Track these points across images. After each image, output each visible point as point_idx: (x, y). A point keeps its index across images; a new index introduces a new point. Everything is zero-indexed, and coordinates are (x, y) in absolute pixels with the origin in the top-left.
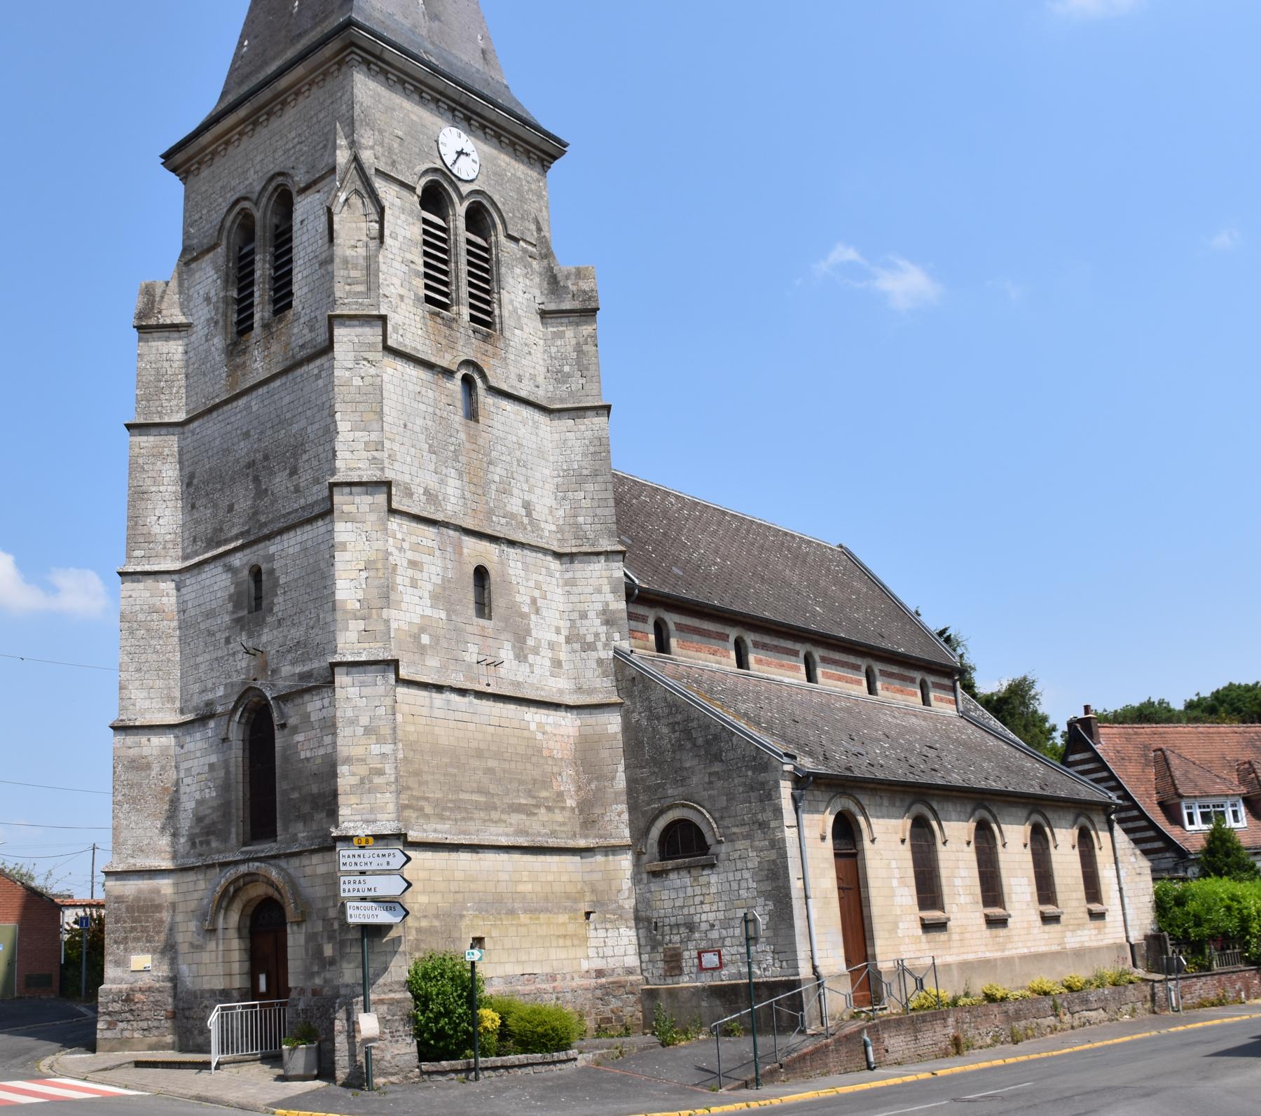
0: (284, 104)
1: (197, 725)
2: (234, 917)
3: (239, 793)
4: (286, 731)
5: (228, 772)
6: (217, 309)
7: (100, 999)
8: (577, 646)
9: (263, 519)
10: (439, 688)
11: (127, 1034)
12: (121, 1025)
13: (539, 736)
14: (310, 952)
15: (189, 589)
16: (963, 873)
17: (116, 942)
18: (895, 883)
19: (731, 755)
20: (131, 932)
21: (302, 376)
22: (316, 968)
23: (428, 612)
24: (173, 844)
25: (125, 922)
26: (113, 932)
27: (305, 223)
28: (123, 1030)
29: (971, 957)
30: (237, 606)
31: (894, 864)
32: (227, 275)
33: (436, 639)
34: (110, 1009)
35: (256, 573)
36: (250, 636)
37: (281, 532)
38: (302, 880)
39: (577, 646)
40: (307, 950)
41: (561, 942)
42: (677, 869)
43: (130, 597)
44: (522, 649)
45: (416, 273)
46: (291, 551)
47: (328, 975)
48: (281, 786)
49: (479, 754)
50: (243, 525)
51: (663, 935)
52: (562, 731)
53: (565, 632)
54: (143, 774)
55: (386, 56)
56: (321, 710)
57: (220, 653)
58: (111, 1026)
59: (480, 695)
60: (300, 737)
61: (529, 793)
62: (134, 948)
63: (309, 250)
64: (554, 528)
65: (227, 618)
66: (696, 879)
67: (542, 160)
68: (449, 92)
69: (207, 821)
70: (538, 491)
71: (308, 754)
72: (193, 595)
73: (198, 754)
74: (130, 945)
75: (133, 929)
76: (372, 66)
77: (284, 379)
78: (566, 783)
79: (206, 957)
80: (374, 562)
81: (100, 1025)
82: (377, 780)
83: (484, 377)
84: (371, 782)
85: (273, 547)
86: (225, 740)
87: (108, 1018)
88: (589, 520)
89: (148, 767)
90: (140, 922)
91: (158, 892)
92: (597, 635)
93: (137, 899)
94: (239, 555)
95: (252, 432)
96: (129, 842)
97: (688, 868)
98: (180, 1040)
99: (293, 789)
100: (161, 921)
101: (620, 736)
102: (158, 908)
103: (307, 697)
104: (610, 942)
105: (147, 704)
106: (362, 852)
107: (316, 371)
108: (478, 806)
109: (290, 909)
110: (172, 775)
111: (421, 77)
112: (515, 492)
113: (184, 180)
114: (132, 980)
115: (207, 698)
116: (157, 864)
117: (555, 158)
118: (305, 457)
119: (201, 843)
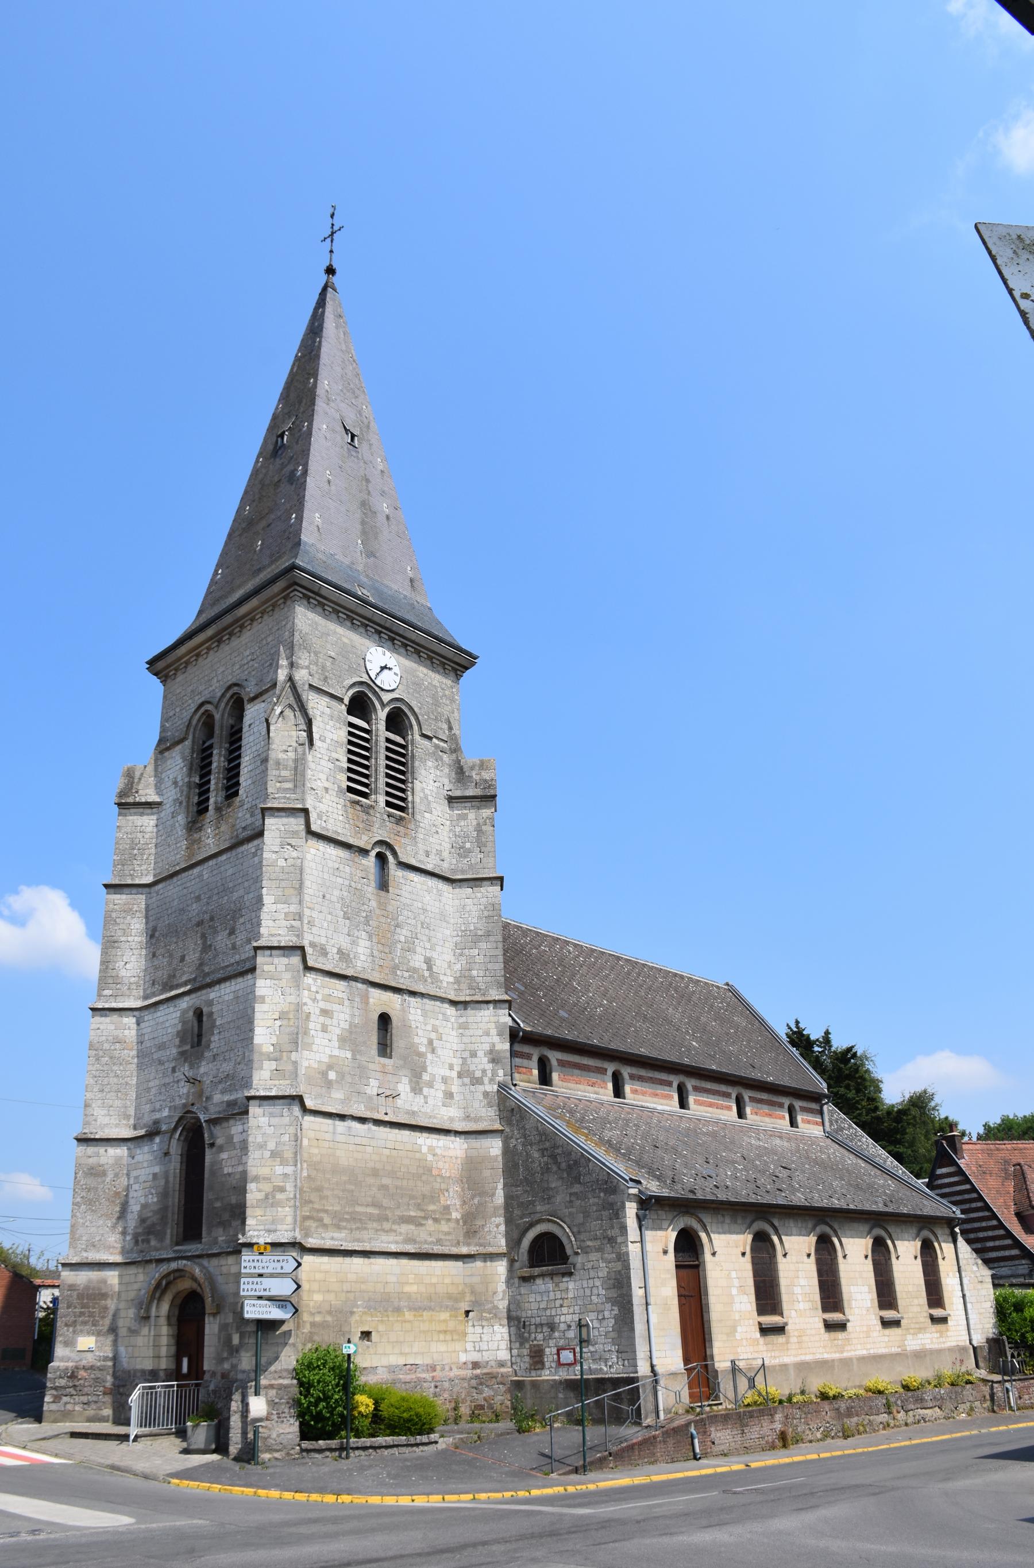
0: (242, 627)
1: (146, 1139)
2: (165, 1307)
3: (175, 1200)
4: (214, 1149)
5: (167, 1182)
6: (182, 792)
7: (49, 1375)
8: (467, 1080)
9: (207, 969)
10: (342, 1117)
11: (69, 1407)
12: (65, 1399)
13: (430, 1158)
15: (147, 1024)
16: (803, 1282)
17: (66, 1325)
18: (734, 1291)
19: (587, 1179)
20: (80, 1316)
21: (242, 852)
22: (225, 1355)
23: (336, 1052)
25: (75, 1307)
26: (65, 1316)
27: (252, 726)
28: (66, 1403)
29: (808, 1358)
30: (183, 1041)
31: (734, 1274)
32: (191, 764)
33: (341, 1075)
34: (57, 1384)
35: (199, 1014)
36: (191, 1067)
37: (220, 981)
38: (219, 1277)
39: (467, 1080)
40: (219, 1338)
41: (442, 1337)
42: (542, 1275)
43: (99, 1029)
44: (418, 1083)
45: (341, 769)
46: (226, 998)
47: (234, 1361)
48: (208, 1195)
49: (375, 1173)
50: (191, 973)
51: (530, 1333)
52: (451, 1153)
53: (457, 1068)
54: (100, 1180)
55: (323, 592)
57: (167, 1080)
58: (57, 1399)
59: (378, 1122)
60: (224, 1156)
61: (419, 1207)
62: (81, 1331)
63: (254, 749)
64: (451, 980)
65: (174, 1051)
66: (557, 1285)
67: (455, 670)
68: (376, 619)
69: (149, 1222)
70: (438, 949)
71: (230, 1170)
72: (149, 1030)
73: (145, 1165)
74: (79, 1327)
75: (82, 1314)
76: (312, 600)
78: (453, 1198)
79: (140, 1341)
80: (287, 1013)
81: (47, 1399)
82: (279, 1196)
83: (394, 853)
84: (274, 1197)
85: (213, 994)
86: (167, 1154)
87: (54, 1392)
88: (482, 973)
89: (104, 1174)
90: (88, 1308)
91: (104, 1281)
92: (484, 1071)
93: (87, 1288)
94: (186, 998)
95: (202, 897)
96: (84, 1238)
97: (551, 1275)
99: (217, 1199)
100: (106, 1308)
101: (500, 1158)
102: (104, 1296)
103: (232, 1122)
104: (485, 1338)
105: (106, 1120)
106: (260, 1257)
107: (253, 850)
108: (371, 1218)
109: (208, 1301)
110: (124, 1181)
111: (353, 608)
112: (419, 949)
113: (164, 682)
114: (77, 1359)
115: (154, 1117)
116: (105, 1258)
117: (467, 668)
118: (242, 920)
119: (143, 1241)
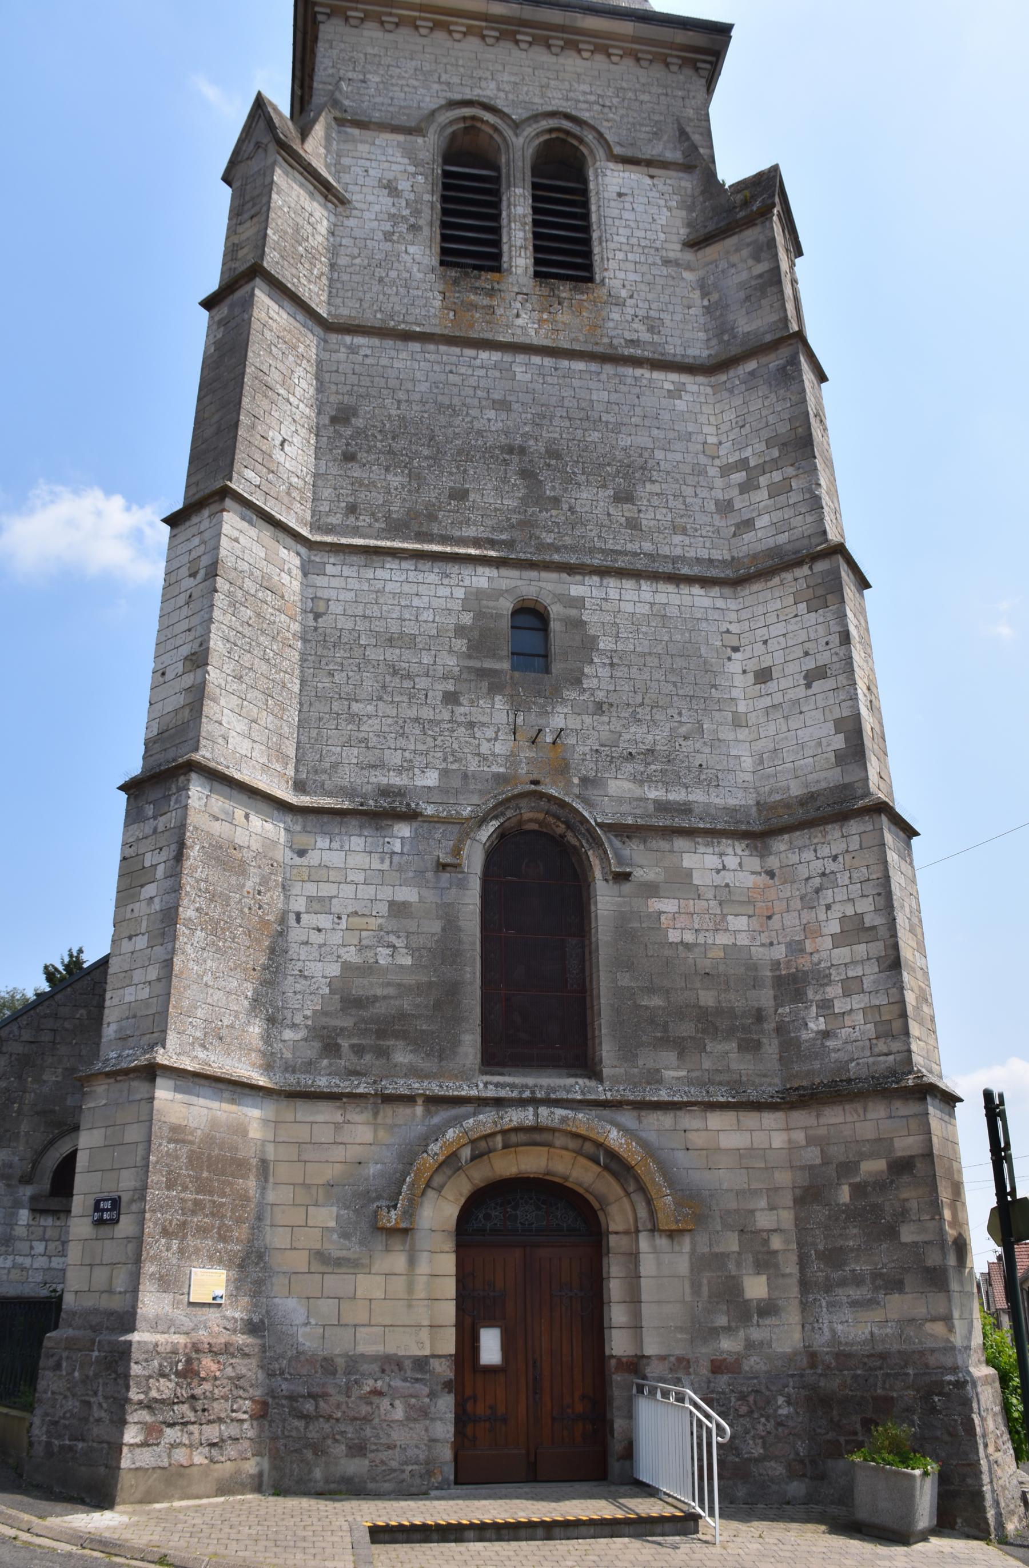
1: (354, 822)
7: (135, 1369)
11: (180, 1456)
12: (171, 1434)
14: (705, 1290)
17: (165, 1232)
20: (194, 1213)
24: (267, 1038)
25: (185, 1188)
26: (162, 1208)
28: (173, 1446)
34: (154, 1394)
38: (680, 1156)
40: (696, 1287)
43: (236, 540)
47: (756, 1334)
54: (233, 880)
56: (718, 871)
58: (151, 1436)
62: (197, 1251)
71: (689, 937)
74: (191, 1242)
75: (198, 1206)
77: (594, 367)
81: (131, 1435)
87: (144, 1416)
89: (241, 869)
90: (211, 1193)
91: (242, 1131)
93: (209, 1140)
96: (200, 1013)
98: (274, 1467)
100: (246, 1198)
102: (240, 1166)
105: (244, 747)
110: (274, 898)
114: (189, 1324)
115: (384, 781)
116: (247, 1074)
